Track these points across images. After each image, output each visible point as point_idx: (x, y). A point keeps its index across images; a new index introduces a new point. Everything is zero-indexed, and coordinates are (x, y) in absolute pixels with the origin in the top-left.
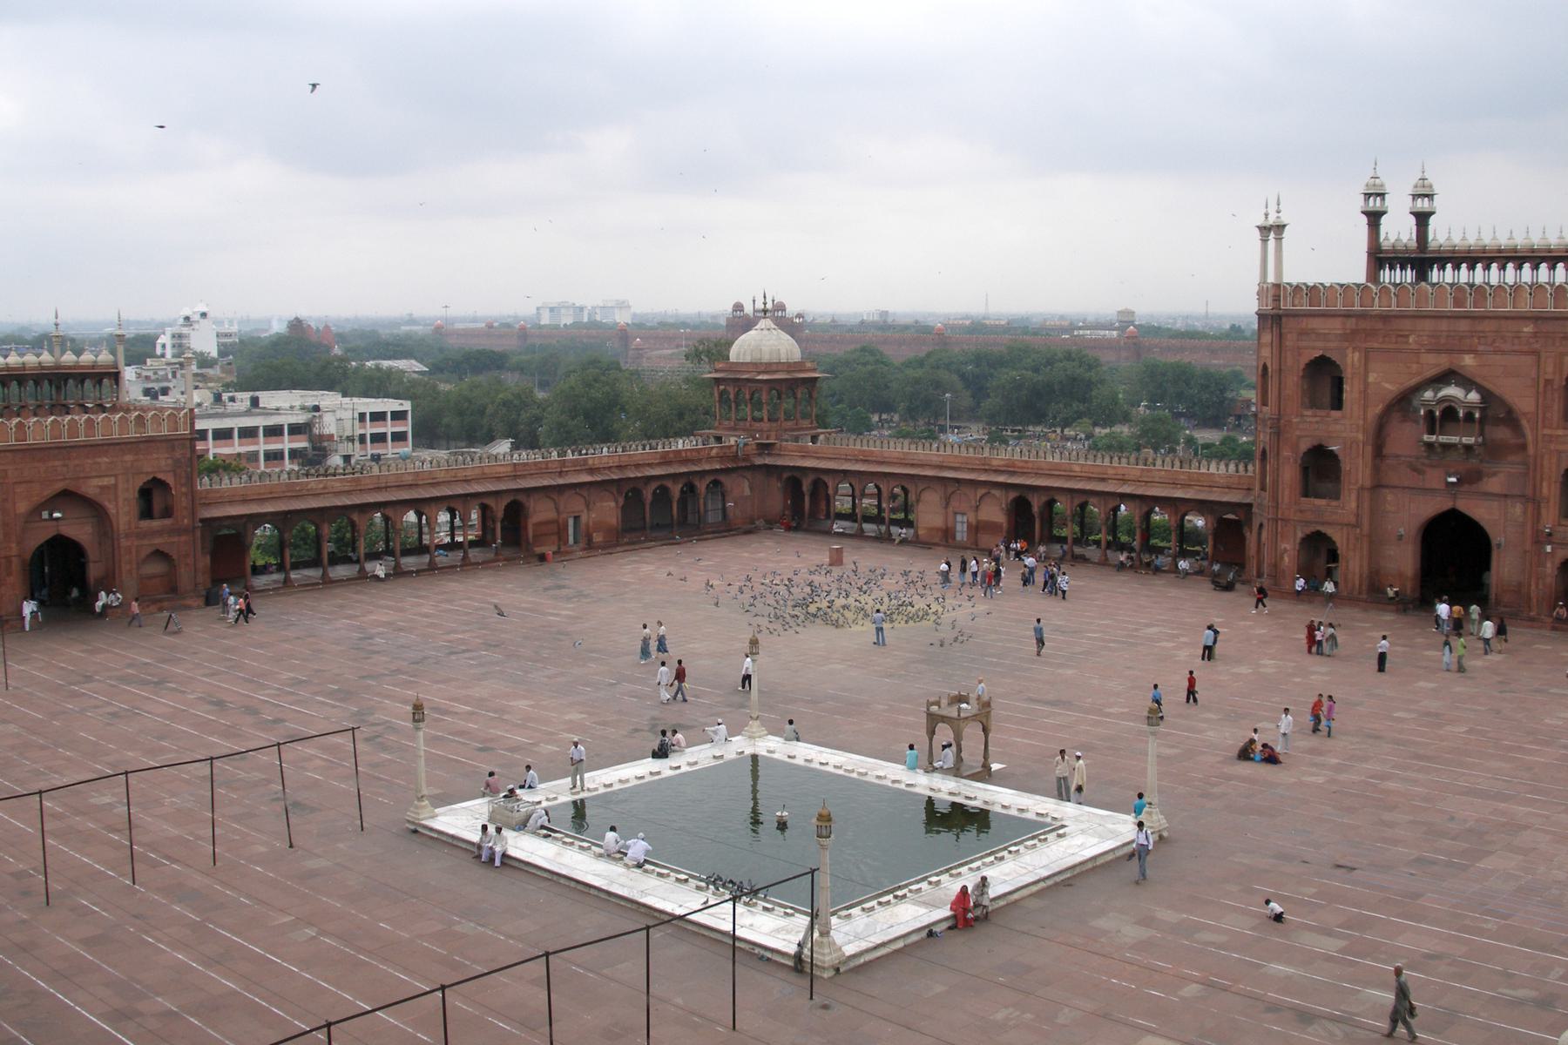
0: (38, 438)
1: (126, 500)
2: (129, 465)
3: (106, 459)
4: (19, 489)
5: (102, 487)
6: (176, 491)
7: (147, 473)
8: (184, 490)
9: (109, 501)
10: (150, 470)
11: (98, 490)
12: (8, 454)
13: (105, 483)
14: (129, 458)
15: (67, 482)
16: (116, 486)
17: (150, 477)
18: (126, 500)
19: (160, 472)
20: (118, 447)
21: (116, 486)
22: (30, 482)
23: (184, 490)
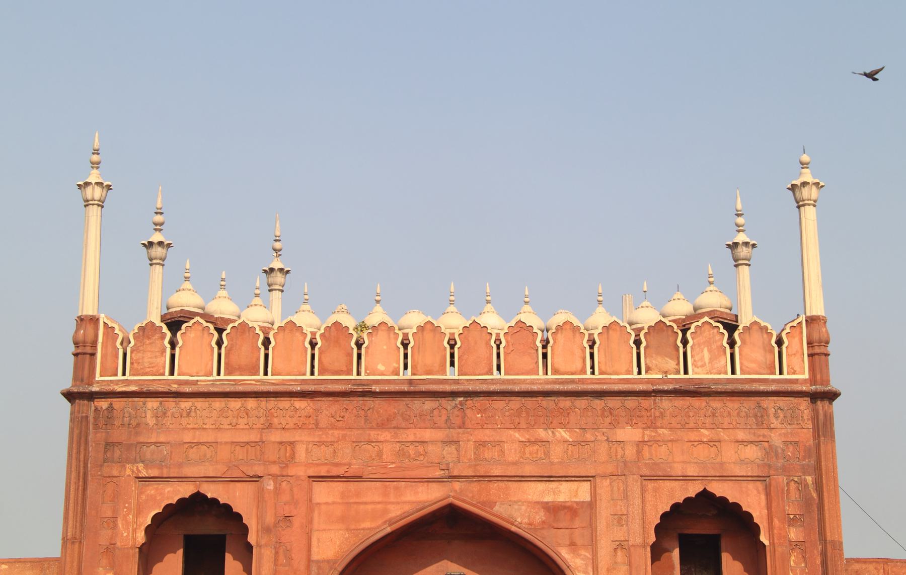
0: (381, 367)
1: (620, 545)
2: (630, 452)
3: (563, 433)
4: (323, 493)
5: (554, 509)
6: (771, 538)
7: (686, 478)
8: (794, 534)
9: (572, 545)
10: (691, 471)
11: (540, 516)
12: (300, 403)
13: (561, 498)
14: (629, 434)
15: (457, 486)
16: (591, 505)
17: (693, 490)
18: (620, 545)
19: (723, 478)
20: (598, 403)
21: (591, 505)
22: (358, 478)
23: (794, 534)
